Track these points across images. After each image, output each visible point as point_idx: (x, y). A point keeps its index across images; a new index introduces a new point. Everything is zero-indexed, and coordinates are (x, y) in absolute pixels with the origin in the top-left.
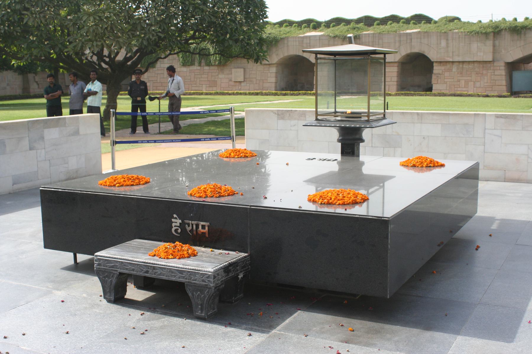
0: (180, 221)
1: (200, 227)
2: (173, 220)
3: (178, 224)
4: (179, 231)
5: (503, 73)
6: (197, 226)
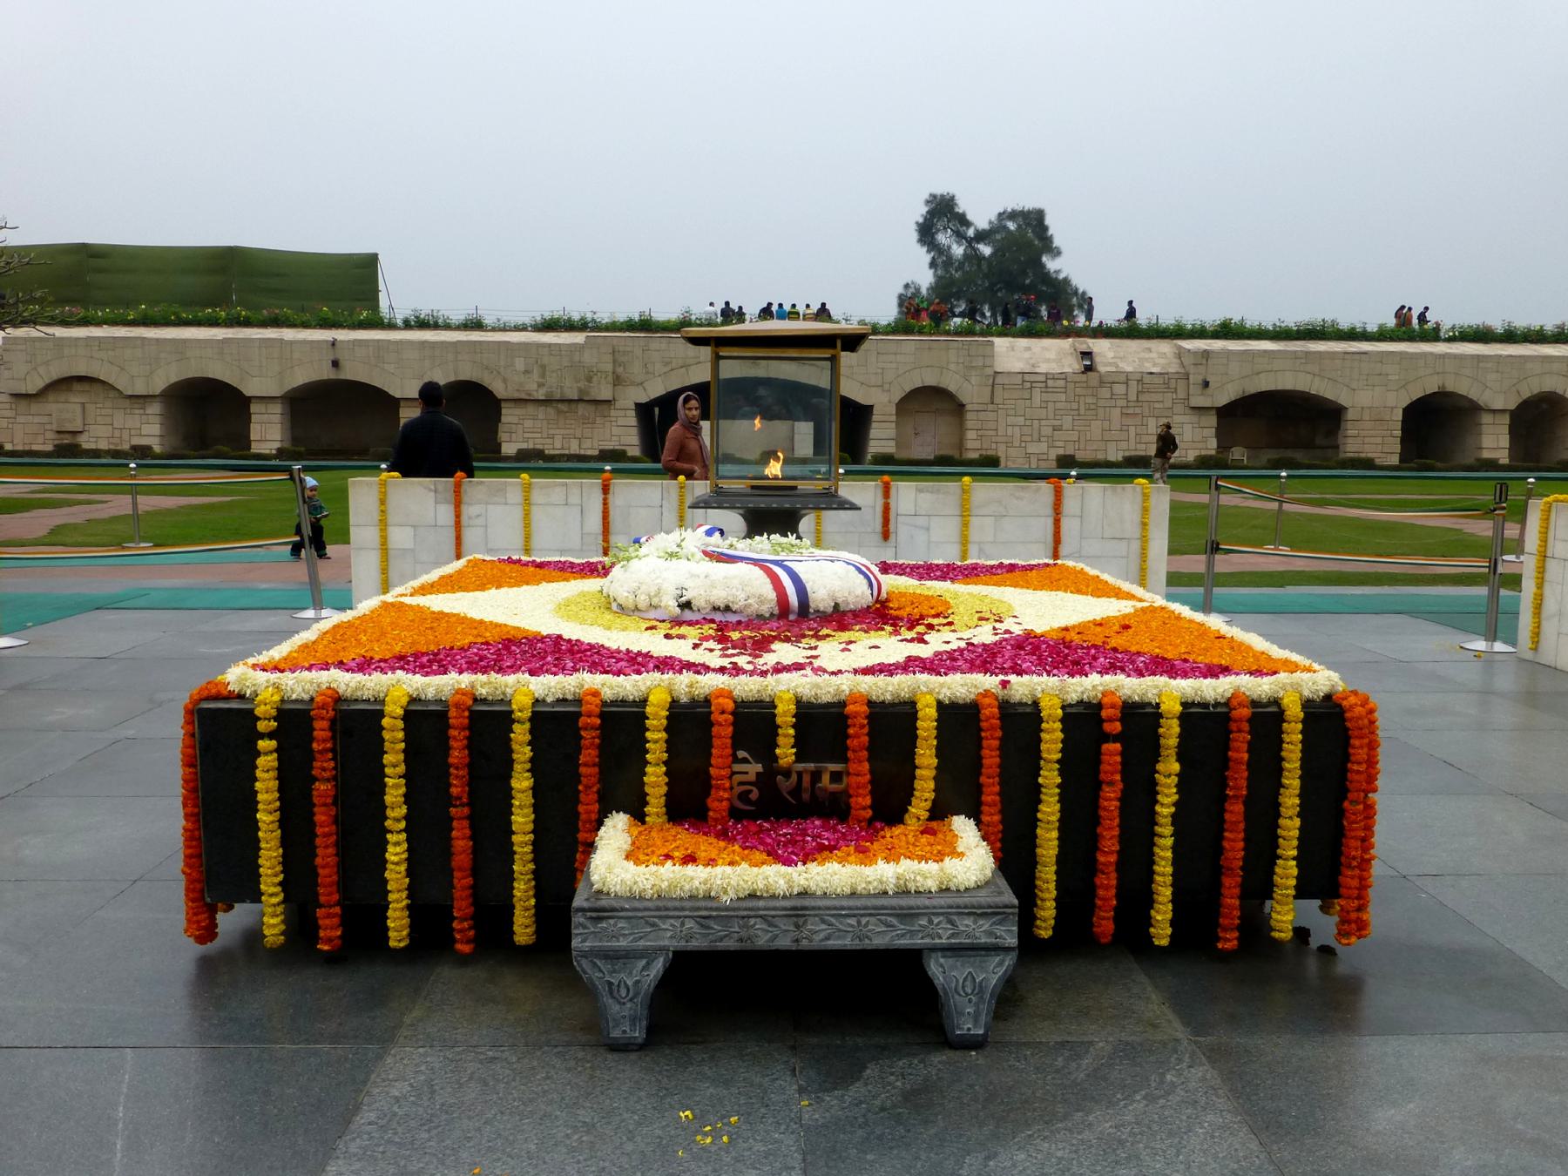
0: (759, 768)
1: (826, 778)
3: (752, 777)
4: (755, 795)
5: (633, 421)
6: (816, 776)
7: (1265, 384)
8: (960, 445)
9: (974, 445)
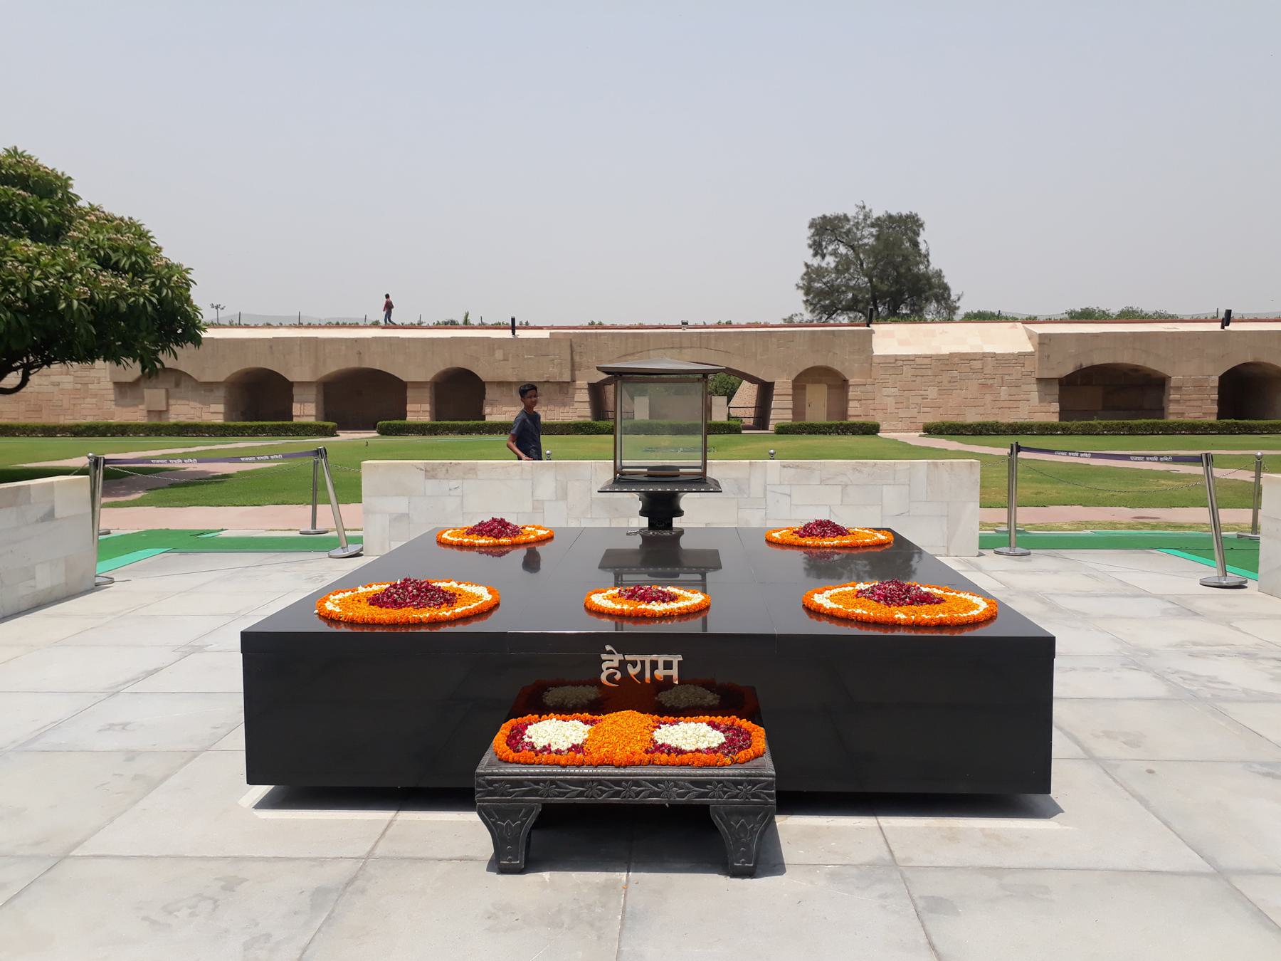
1: (661, 665)
2: (604, 657)
3: (616, 664)
4: (618, 676)
5: (586, 397)
6: (654, 665)
7: (1098, 359)
8: (844, 414)
9: (856, 411)
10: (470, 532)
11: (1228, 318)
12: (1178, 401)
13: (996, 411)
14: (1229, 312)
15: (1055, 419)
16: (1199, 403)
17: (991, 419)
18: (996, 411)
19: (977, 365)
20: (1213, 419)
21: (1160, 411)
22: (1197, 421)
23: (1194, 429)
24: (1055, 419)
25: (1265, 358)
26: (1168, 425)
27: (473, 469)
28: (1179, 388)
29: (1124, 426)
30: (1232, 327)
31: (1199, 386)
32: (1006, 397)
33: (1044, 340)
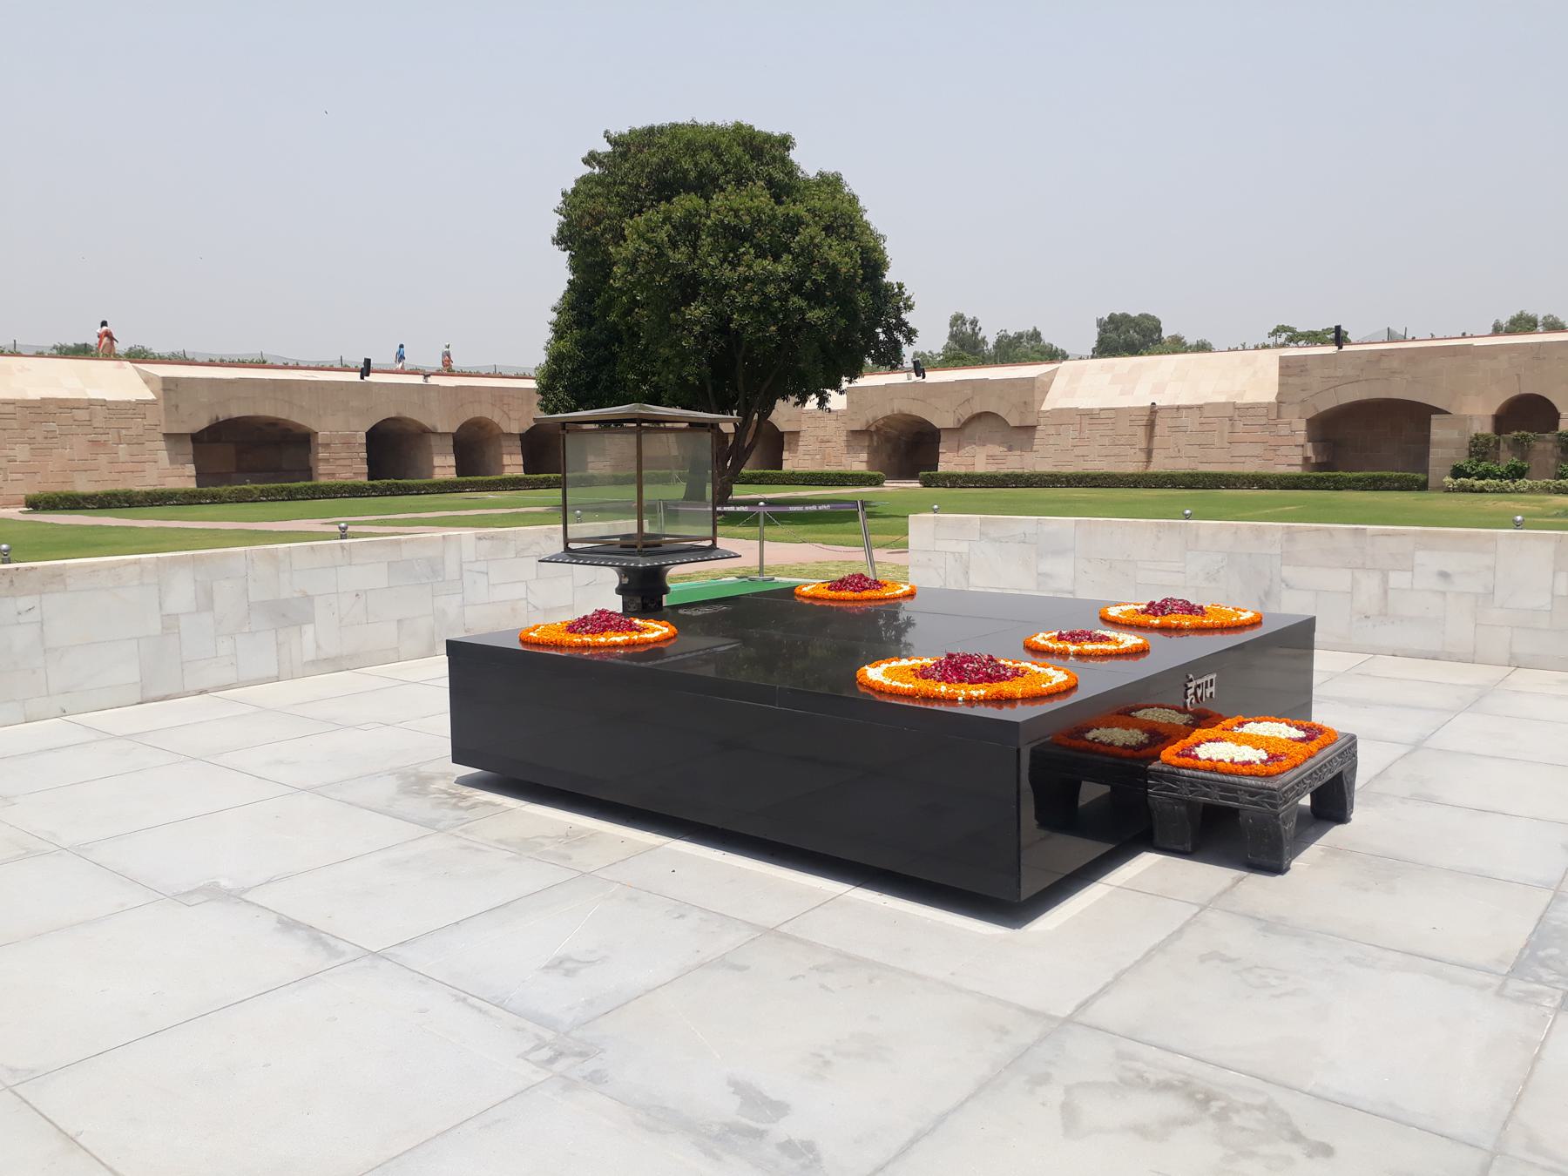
7: (236, 411)
10: (571, 628)
11: (366, 369)
12: (327, 460)
13: (116, 476)
14: (368, 362)
15: (192, 485)
16: (348, 462)
17: (120, 487)
18: (116, 476)
19: (82, 415)
20: (364, 480)
21: (308, 473)
22: (349, 482)
23: (355, 491)
24: (192, 485)
25: (407, 414)
26: (316, 487)
27: (58, 576)
28: (327, 445)
29: (283, 489)
30: (373, 378)
31: (347, 443)
32: (128, 458)
33: (169, 385)
